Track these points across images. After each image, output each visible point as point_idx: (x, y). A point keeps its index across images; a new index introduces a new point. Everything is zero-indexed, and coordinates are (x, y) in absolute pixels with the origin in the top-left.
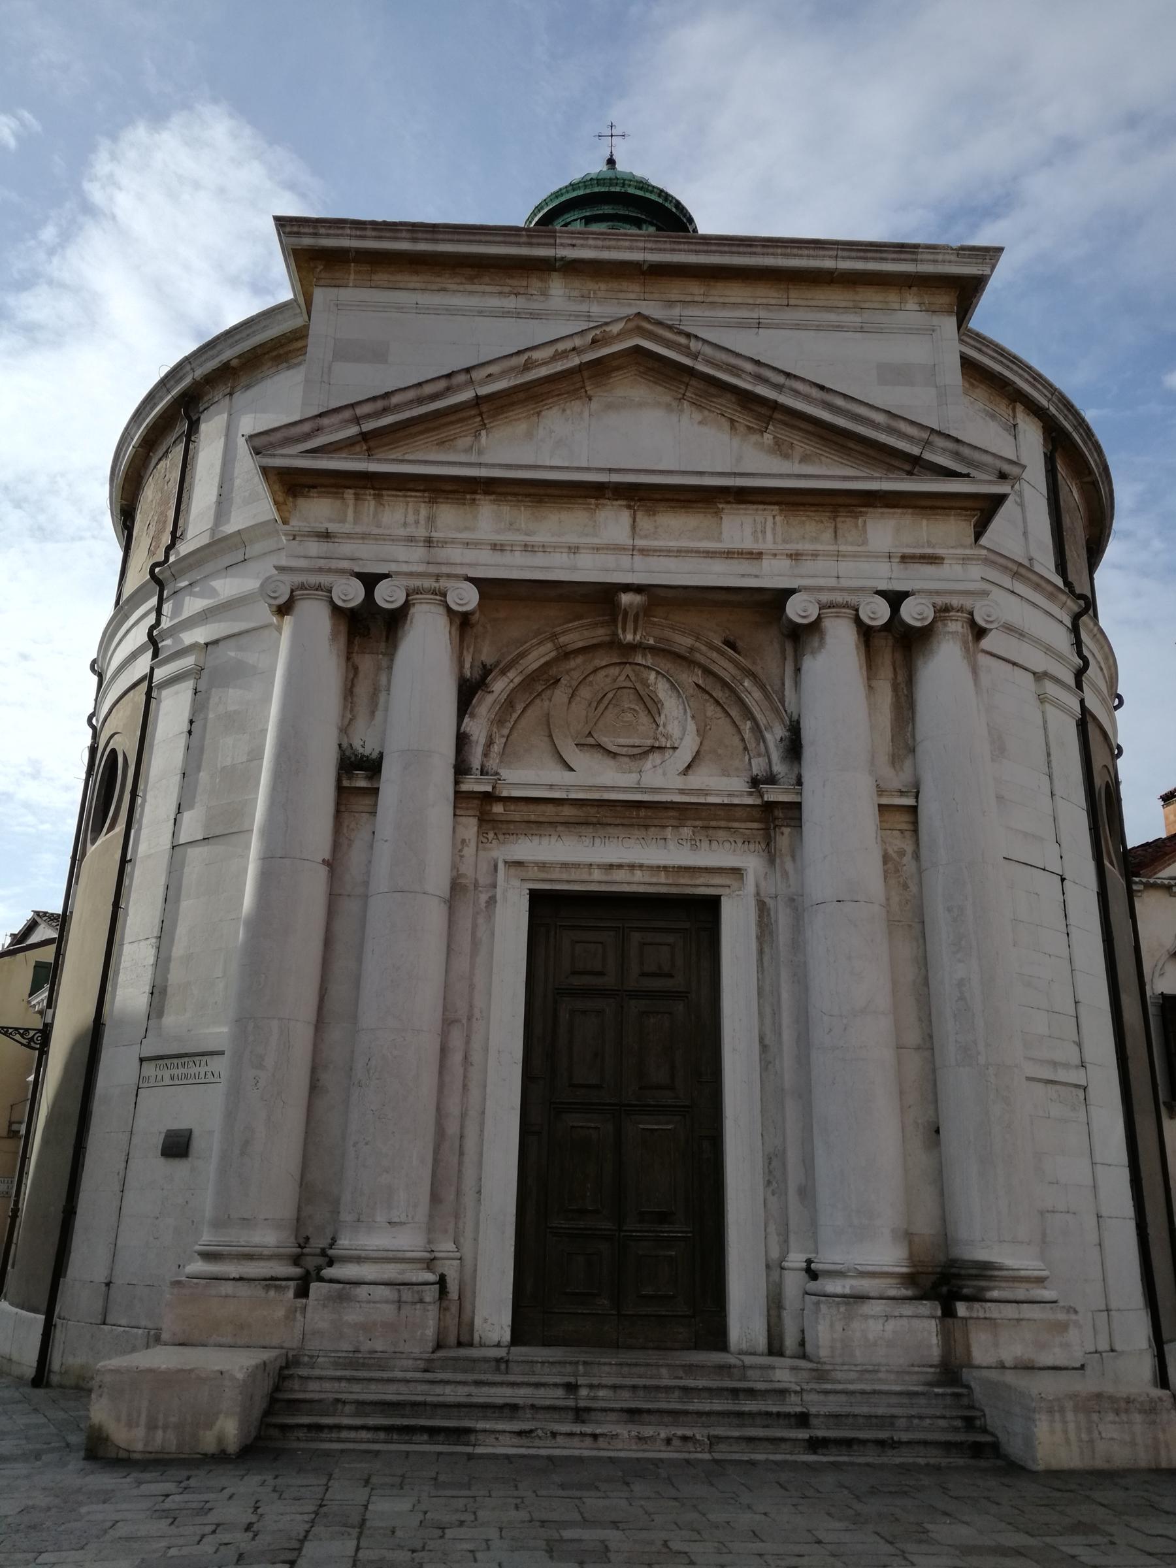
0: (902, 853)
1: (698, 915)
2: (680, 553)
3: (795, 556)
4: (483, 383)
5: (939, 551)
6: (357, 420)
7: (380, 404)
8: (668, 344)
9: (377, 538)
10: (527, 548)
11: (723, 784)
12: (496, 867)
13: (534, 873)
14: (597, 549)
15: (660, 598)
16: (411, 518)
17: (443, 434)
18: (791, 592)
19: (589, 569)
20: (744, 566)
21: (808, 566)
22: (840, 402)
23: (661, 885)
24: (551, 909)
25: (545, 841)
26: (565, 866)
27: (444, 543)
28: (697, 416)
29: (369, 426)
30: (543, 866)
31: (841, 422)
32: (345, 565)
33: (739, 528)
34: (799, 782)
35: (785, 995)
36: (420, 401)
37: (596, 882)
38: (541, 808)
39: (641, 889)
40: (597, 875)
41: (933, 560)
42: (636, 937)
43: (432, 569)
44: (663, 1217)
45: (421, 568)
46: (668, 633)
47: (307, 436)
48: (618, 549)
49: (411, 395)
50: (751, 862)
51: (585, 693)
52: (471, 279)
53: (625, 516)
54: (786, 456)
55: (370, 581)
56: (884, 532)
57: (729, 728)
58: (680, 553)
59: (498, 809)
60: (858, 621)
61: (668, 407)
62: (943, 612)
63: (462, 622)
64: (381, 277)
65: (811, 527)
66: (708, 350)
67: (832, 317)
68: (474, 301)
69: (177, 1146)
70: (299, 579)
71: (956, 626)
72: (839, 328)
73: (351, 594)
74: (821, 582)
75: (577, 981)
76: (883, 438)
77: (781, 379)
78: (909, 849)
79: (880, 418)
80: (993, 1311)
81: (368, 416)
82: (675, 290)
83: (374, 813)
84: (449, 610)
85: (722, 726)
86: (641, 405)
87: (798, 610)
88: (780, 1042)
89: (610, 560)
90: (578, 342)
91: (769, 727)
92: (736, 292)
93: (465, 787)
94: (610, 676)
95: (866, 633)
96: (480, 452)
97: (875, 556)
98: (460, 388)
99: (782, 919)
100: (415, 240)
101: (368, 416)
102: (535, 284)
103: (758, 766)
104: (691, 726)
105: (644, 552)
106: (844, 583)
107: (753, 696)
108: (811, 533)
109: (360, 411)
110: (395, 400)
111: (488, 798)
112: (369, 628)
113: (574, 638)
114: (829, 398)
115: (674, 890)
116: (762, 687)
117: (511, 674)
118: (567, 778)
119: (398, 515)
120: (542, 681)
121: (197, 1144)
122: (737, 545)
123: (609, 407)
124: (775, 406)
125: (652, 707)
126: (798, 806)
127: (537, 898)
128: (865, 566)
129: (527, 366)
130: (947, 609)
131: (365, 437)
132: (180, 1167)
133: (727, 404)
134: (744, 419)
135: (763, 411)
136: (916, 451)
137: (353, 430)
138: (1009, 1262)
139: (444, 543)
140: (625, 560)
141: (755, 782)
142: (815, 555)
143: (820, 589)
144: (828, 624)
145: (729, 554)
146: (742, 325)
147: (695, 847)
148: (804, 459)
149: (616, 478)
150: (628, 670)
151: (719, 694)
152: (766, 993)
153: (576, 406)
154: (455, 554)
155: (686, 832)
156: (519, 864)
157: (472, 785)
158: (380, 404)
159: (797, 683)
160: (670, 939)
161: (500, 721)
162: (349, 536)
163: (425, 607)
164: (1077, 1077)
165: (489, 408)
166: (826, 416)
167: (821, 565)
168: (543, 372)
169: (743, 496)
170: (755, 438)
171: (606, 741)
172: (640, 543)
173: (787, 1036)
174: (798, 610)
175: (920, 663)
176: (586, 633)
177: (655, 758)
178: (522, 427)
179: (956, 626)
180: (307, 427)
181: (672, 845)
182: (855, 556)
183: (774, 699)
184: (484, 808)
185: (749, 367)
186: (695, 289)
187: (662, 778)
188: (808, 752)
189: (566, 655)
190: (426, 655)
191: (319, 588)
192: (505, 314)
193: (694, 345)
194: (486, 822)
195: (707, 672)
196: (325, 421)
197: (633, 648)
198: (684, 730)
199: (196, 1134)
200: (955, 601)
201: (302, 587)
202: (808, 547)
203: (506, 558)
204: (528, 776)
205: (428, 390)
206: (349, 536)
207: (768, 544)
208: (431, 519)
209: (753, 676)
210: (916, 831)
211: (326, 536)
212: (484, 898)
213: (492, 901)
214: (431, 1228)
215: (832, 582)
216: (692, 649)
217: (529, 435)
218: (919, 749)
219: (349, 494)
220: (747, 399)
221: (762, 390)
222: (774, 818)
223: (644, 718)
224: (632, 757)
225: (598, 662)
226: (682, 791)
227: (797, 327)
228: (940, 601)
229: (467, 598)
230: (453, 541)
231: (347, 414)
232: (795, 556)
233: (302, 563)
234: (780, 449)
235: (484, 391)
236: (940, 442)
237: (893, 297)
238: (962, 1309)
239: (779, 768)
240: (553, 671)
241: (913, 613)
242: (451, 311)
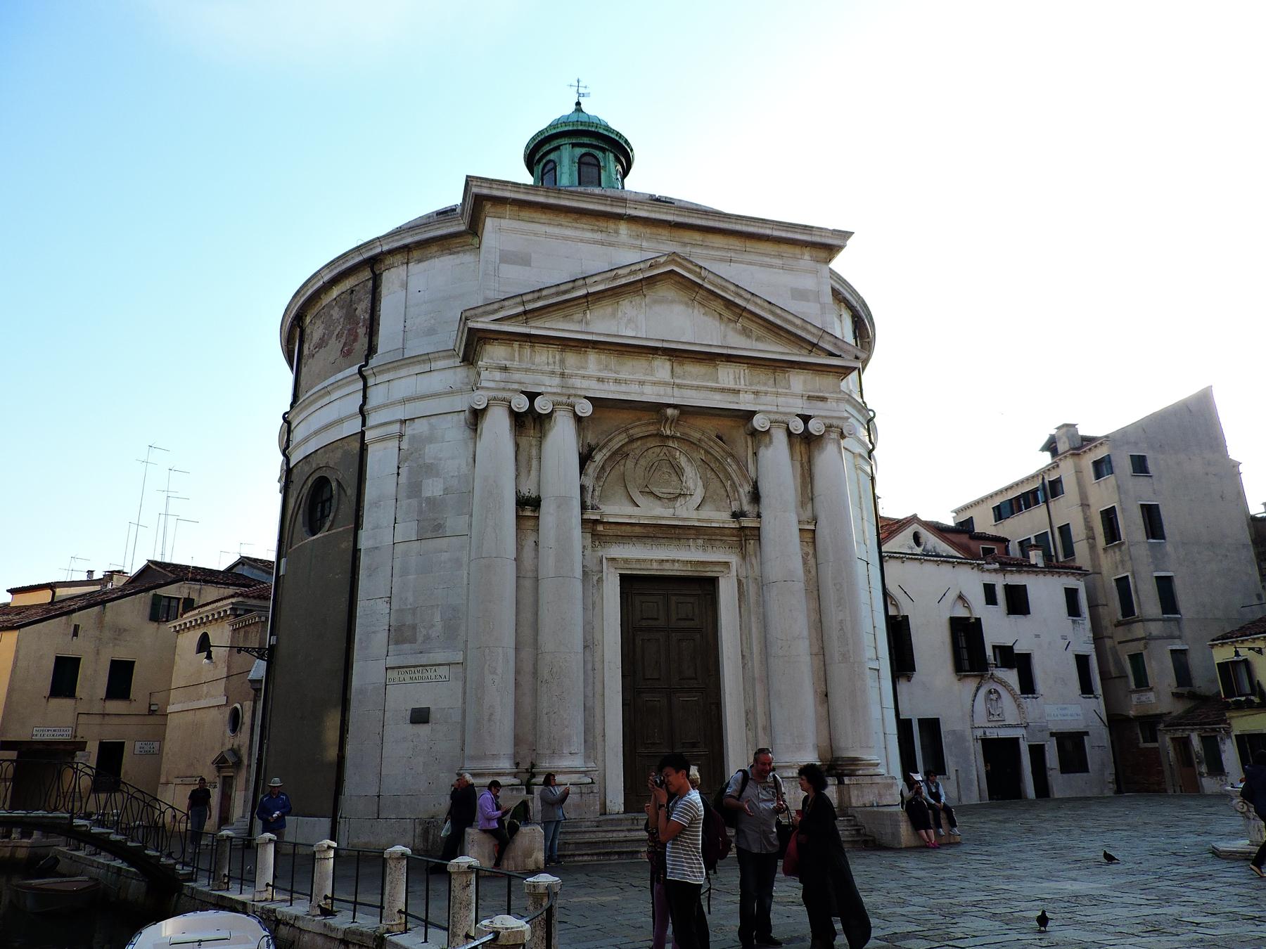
0: (807, 554)
1: (704, 587)
2: (698, 388)
3: (756, 393)
4: (591, 286)
5: (827, 395)
6: (523, 303)
7: (536, 295)
8: (689, 271)
9: (534, 371)
10: (617, 381)
11: (719, 517)
12: (601, 561)
13: (621, 565)
14: (654, 383)
15: (686, 411)
16: (551, 360)
17: (567, 312)
18: (754, 413)
19: (650, 394)
20: (731, 397)
21: (763, 399)
22: (779, 311)
23: (688, 571)
24: (629, 583)
25: (626, 546)
26: (638, 560)
27: (571, 376)
28: (702, 311)
29: (530, 307)
30: (626, 561)
31: (779, 322)
32: (516, 386)
33: (727, 375)
34: (759, 516)
35: (754, 630)
36: (558, 294)
37: (655, 570)
38: (624, 528)
39: (678, 573)
40: (655, 566)
41: (823, 399)
42: (674, 599)
43: (564, 391)
44: (694, 745)
45: (559, 391)
46: (687, 430)
47: (496, 311)
48: (666, 384)
49: (553, 290)
50: (734, 559)
51: (642, 462)
52: (575, 220)
53: (668, 364)
54: (749, 337)
55: (532, 396)
56: (798, 382)
57: (719, 484)
58: (698, 388)
59: (600, 528)
60: (788, 430)
61: (687, 304)
62: (829, 427)
63: (579, 419)
64: (525, 214)
65: (763, 377)
66: (711, 277)
67: (767, 259)
68: (578, 233)
69: (420, 716)
70: (492, 394)
71: (834, 436)
72: (771, 266)
73: (521, 404)
74: (769, 408)
75: (644, 623)
76: (799, 332)
77: (749, 296)
78: (811, 552)
79: (798, 322)
80: (861, 780)
81: (529, 301)
82: (688, 236)
83: (536, 530)
84: (575, 414)
85: (715, 484)
86: (672, 302)
87: (759, 422)
88: (752, 653)
89: (661, 390)
90: (642, 266)
91: (741, 485)
92: (718, 241)
93: (585, 517)
94: (655, 453)
95: (790, 434)
96: (587, 323)
97: (794, 395)
98: (580, 288)
99: (752, 590)
100: (547, 196)
101: (529, 301)
102: (611, 225)
103: (735, 507)
104: (700, 483)
105: (679, 386)
106: (781, 409)
107: (732, 468)
108: (762, 380)
109: (525, 298)
110: (544, 293)
111: (596, 522)
112: (529, 423)
113: (637, 432)
114: (773, 308)
115: (696, 574)
116: (738, 463)
117: (604, 451)
118: (629, 509)
119: (544, 357)
120: (619, 455)
121: (432, 716)
122: (726, 386)
123: (655, 302)
124: (745, 309)
125: (678, 471)
126: (759, 528)
127: (624, 578)
128: (791, 400)
129: (615, 278)
130: (831, 426)
131: (525, 312)
132: (423, 729)
133: (718, 306)
134: (727, 314)
135: (738, 311)
136: (815, 341)
137: (521, 309)
138: (865, 757)
139: (571, 376)
140: (669, 390)
141: (735, 515)
142: (766, 393)
143: (769, 412)
144: (773, 431)
145: (723, 390)
146: (722, 260)
147: (704, 550)
149: (666, 345)
150: (665, 450)
151: (712, 467)
152: (744, 629)
154: (578, 382)
155: (700, 542)
156: (613, 559)
157: (591, 515)
158: (536, 295)
159: (756, 461)
160: (692, 600)
161: (598, 478)
162: (518, 370)
163: (562, 413)
165: (592, 299)
166: (771, 318)
167: (769, 398)
168: (624, 281)
170: (732, 325)
171: (655, 490)
172: (677, 381)
173: (756, 649)
174: (759, 422)
175: (816, 453)
176: (644, 429)
177: (681, 501)
178: (609, 310)
179: (834, 436)
180: (496, 306)
181: (693, 549)
182: (786, 394)
183: (742, 467)
184: (592, 527)
185: (732, 288)
186: (697, 237)
187: (685, 512)
188: (764, 501)
189: (632, 440)
190: (562, 440)
191: (504, 400)
192: (595, 242)
193: (704, 273)
194: (596, 536)
195: (707, 452)
196: (506, 303)
197: (668, 437)
198: (696, 485)
199: (432, 709)
200: (835, 422)
201: (495, 399)
202: (763, 389)
203: (605, 386)
204: (616, 510)
205: (563, 288)
206: (518, 370)
207: (742, 386)
208: (562, 361)
209: (732, 456)
210: (814, 542)
211: (505, 369)
212: (595, 578)
213: (600, 580)
214: (587, 757)
215: (775, 409)
216: (700, 440)
217: (614, 315)
218: (816, 500)
219: (516, 345)
220: (729, 304)
221: (738, 301)
222: (746, 536)
223: (675, 478)
224: (669, 499)
225: (649, 445)
226: (699, 520)
227: (750, 264)
228: (828, 422)
229: (585, 409)
230: (576, 375)
231: (518, 300)
232: (756, 393)
233: (492, 385)
234: (746, 332)
235: (592, 290)
236: (828, 338)
237: (797, 251)
238: (846, 780)
240: (625, 449)
241: (815, 427)
242: (566, 238)
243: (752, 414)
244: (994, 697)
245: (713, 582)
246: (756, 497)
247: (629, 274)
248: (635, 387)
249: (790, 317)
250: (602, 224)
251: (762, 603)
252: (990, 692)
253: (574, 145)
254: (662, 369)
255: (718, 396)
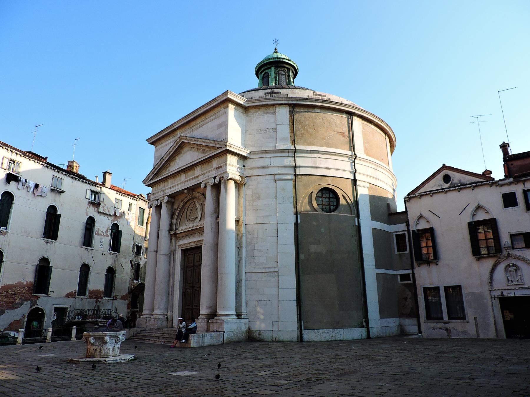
3: (203, 174)
13: (181, 246)
20: (197, 179)
24: (185, 252)
36: (159, 166)
51: (189, 209)
72: (212, 120)
123: (184, 154)
129: (169, 153)
134: (199, 148)
153: (180, 156)
164: (276, 270)
166: (203, 144)
169: (196, 165)
189: (186, 203)
227: (207, 123)
232: (203, 174)
244: (513, 269)
247: (172, 149)
249: (206, 141)
252: (508, 266)
253: (261, 73)
254: (183, 177)
255: (194, 181)
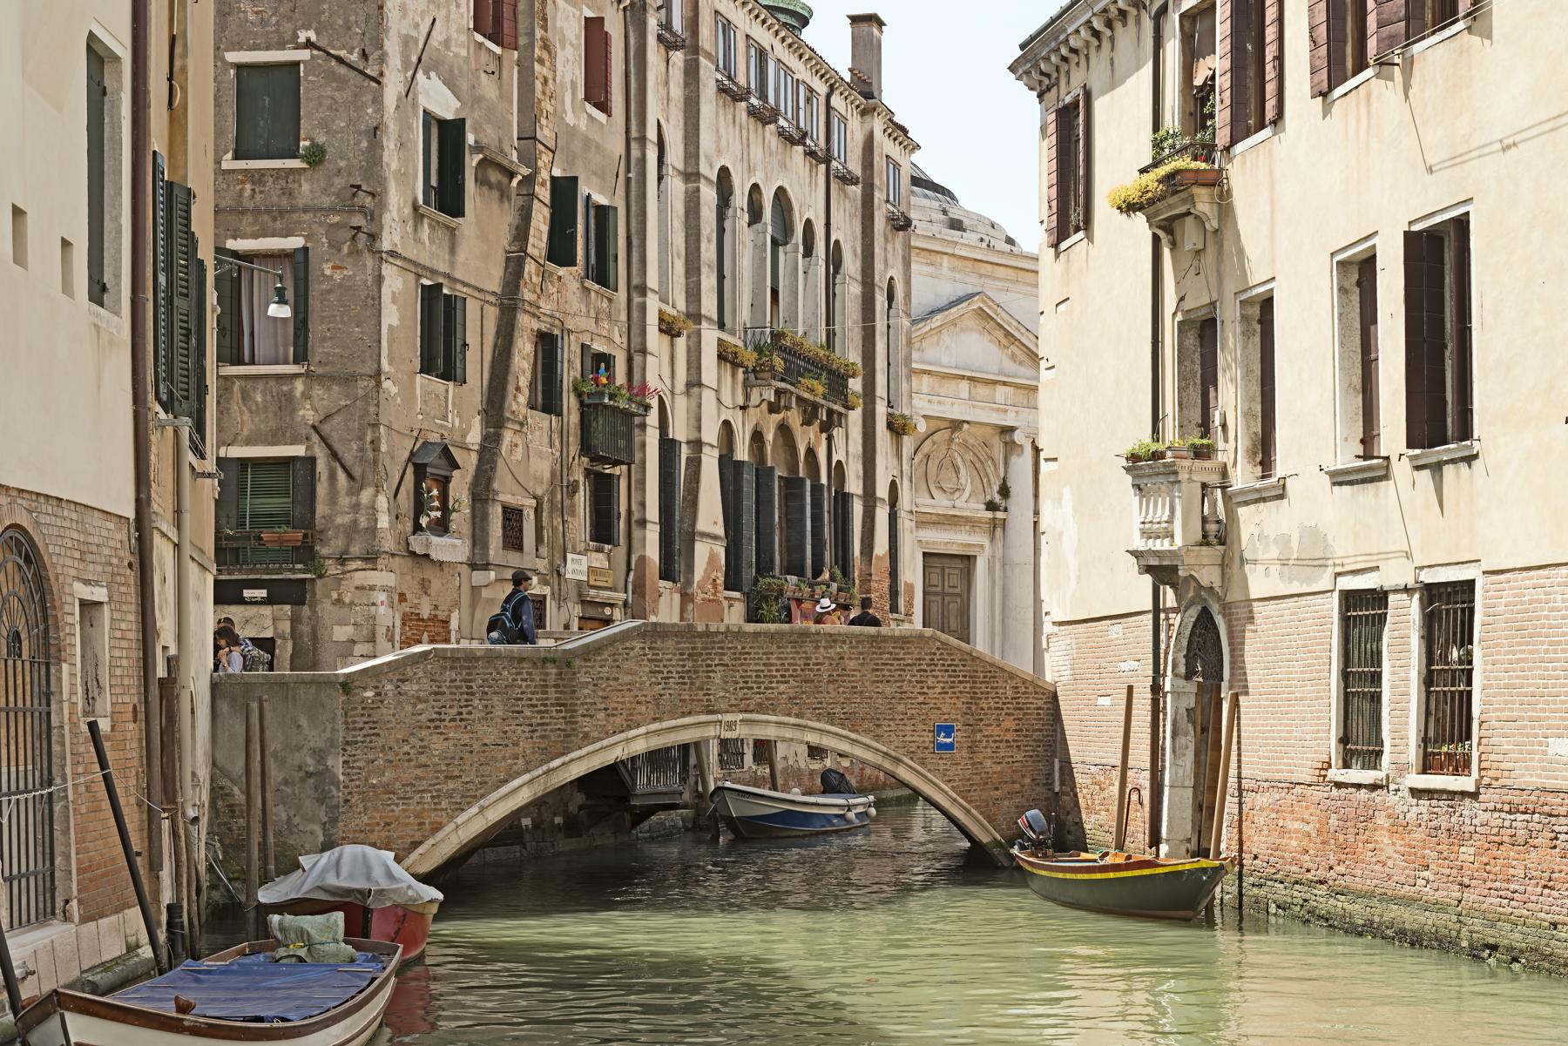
1: (967, 561)
19: (957, 415)
20: (1002, 415)
34: (1006, 510)
87: (1018, 437)
92: (1001, 272)
103: (988, 498)
107: (990, 470)
123: (962, 330)
133: (1000, 334)
134: (1004, 341)
148: (1021, 363)
169: (1005, 384)
178: (935, 338)
220: (1008, 334)
234: (1013, 357)
239: (997, 499)
243: (1012, 429)
245: (969, 560)
246: (1005, 491)
248: (948, 407)
250: (933, 257)
251: (1005, 577)
255: (995, 415)
